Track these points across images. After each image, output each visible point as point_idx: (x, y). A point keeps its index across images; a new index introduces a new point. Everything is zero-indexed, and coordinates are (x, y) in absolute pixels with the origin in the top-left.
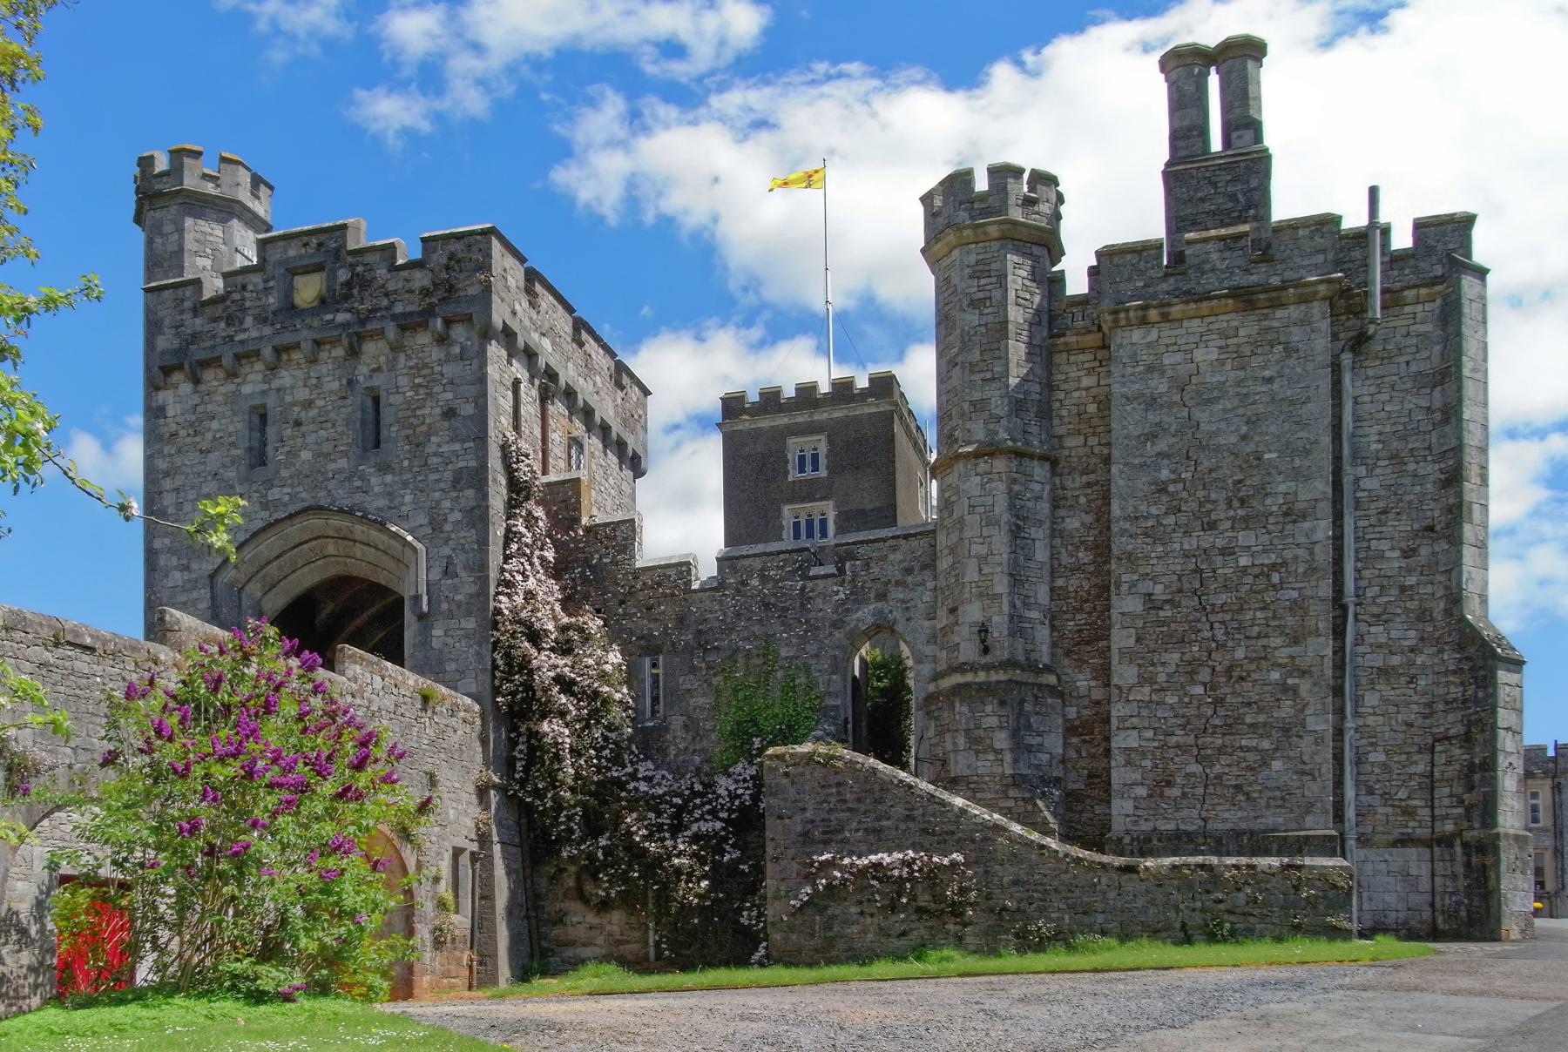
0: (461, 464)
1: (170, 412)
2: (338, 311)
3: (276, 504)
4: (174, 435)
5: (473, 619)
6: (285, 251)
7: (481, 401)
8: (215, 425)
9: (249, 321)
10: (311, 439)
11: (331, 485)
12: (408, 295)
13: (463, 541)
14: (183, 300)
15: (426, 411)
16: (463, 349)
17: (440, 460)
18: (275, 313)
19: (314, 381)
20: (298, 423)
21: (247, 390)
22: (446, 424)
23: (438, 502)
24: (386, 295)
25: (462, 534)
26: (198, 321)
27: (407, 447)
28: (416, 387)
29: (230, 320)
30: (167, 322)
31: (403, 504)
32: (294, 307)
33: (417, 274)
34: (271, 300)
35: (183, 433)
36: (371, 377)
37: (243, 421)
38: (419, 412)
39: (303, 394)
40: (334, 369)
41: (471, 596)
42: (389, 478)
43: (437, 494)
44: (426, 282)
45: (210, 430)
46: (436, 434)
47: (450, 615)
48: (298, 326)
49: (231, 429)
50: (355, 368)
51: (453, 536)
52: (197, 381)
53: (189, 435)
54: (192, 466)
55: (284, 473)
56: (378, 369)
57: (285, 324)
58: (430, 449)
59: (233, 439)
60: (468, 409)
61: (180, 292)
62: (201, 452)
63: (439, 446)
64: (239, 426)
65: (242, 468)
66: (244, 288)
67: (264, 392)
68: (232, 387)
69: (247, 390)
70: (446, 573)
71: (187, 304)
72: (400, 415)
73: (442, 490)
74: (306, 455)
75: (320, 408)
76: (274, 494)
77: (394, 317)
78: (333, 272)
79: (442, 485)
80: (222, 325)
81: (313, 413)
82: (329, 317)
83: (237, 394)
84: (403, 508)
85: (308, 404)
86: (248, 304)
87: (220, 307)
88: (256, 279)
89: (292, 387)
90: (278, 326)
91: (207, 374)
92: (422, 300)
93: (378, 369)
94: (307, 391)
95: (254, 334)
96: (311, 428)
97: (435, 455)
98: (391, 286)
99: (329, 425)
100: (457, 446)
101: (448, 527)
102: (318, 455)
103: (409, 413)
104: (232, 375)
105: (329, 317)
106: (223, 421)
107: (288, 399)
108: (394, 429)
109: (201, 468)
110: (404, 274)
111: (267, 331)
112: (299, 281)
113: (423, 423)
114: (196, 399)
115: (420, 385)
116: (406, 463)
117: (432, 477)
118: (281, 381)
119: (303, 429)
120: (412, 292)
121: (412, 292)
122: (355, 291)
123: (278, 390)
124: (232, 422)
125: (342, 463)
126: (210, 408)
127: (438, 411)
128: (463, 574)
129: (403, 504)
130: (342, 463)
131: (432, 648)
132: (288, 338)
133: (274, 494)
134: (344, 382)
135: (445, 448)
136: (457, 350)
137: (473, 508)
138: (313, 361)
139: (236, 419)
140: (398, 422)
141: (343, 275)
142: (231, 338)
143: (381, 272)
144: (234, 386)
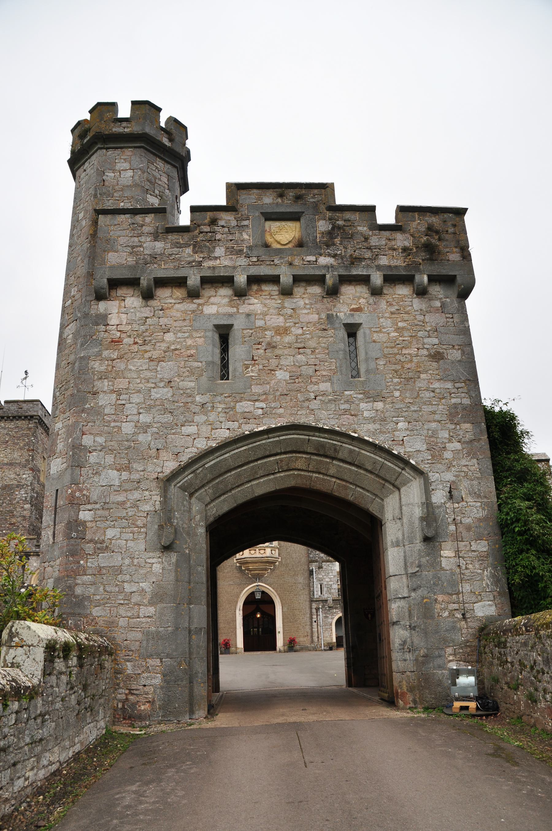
0: (453, 401)
1: (113, 320)
2: (321, 255)
3: (247, 417)
4: (116, 342)
5: (484, 543)
6: (260, 199)
7: (467, 349)
8: (169, 337)
9: (219, 251)
10: (287, 361)
11: (315, 404)
12: (391, 252)
13: (465, 469)
14: (142, 226)
15: (413, 351)
16: (443, 305)
17: (432, 394)
18: (250, 248)
19: (290, 312)
20: (271, 346)
21: (210, 310)
22: (434, 364)
23: (435, 432)
24: (369, 248)
25: (464, 462)
26: (159, 245)
27: (396, 380)
28: (398, 330)
29: (197, 248)
30: (122, 240)
31: (396, 430)
32: (267, 246)
33: (399, 236)
34: (245, 236)
35: (126, 340)
36: (352, 315)
37: (205, 337)
38: (404, 351)
39: (279, 321)
40: (311, 304)
41: (480, 520)
42: (379, 405)
43: (434, 425)
44: (407, 244)
45: (163, 341)
46: (426, 372)
47: (457, 538)
48: (276, 262)
49: (189, 342)
50: (335, 306)
51: (454, 463)
52: (148, 296)
53: (136, 343)
54: (138, 371)
55: (256, 389)
56: (359, 310)
57: (263, 258)
58: (420, 384)
59: (192, 352)
60: (455, 355)
61: (139, 218)
62: (151, 359)
63: (429, 382)
64: (200, 341)
65: (204, 379)
66: (213, 222)
67: (231, 315)
68: (193, 306)
69: (210, 310)
70: (451, 496)
71: (146, 229)
72: (386, 351)
73: (439, 422)
74: (280, 375)
75: (297, 336)
76: (244, 406)
77: (379, 268)
78: (313, 221)
79: (437, 417)
80: (189, 250)
81: (288, 339)
82: (313, 258)
83: (197, 313)
84: (396, 433)
85: (283, 331)
86: (218, 237)
87: (186, 236)
88: (226, 218)
89: (265, 314)
90: (255, 259)
91: (164, 293)
92: (406, 257)
93: (359, 310)
94: (281, 319)
95: (227, 263)
96: (286, 352)
97: (427, 390)
98: (374, 241)
99: (308, 351)
100: (449, 385)
101: (448, 455)
102: (294, 377)
103: (396, 351)
104: (193, 294)
105: (313, 258)
106: (180, 335)
107: (259, 323)
108: (382, 363)
109: (148, 374)
110: (387, 234)
111: (242, 261)
112: (274, 226)
113: (411, 361)
114: (147, 312)
115: (403, 328)
116: (397, 394)
117: (427, 409)
118: (252, 307)
119: (278, 352)
120: (394, 249)
121: (394, 249)
122: (337, 241)
123: (248, 315)
124: (190, 336)
125: (325, 386)
126: (163, 321)
127: (425, 352)
128: (470, 499)
129: (396, 430)
130: (325, 386)
131: (442, 569)
132: (264, 270)
133: (244, 406)
134: (323, 316)
135: (436, 385)
136: (438, 304)
137: (471, 441)
138: (287, 293)
139: (195, 334)
140: (385, 356)
141: (323, 226)
142: (200, 263)
143: (363, 229)
144: (196, 306)
